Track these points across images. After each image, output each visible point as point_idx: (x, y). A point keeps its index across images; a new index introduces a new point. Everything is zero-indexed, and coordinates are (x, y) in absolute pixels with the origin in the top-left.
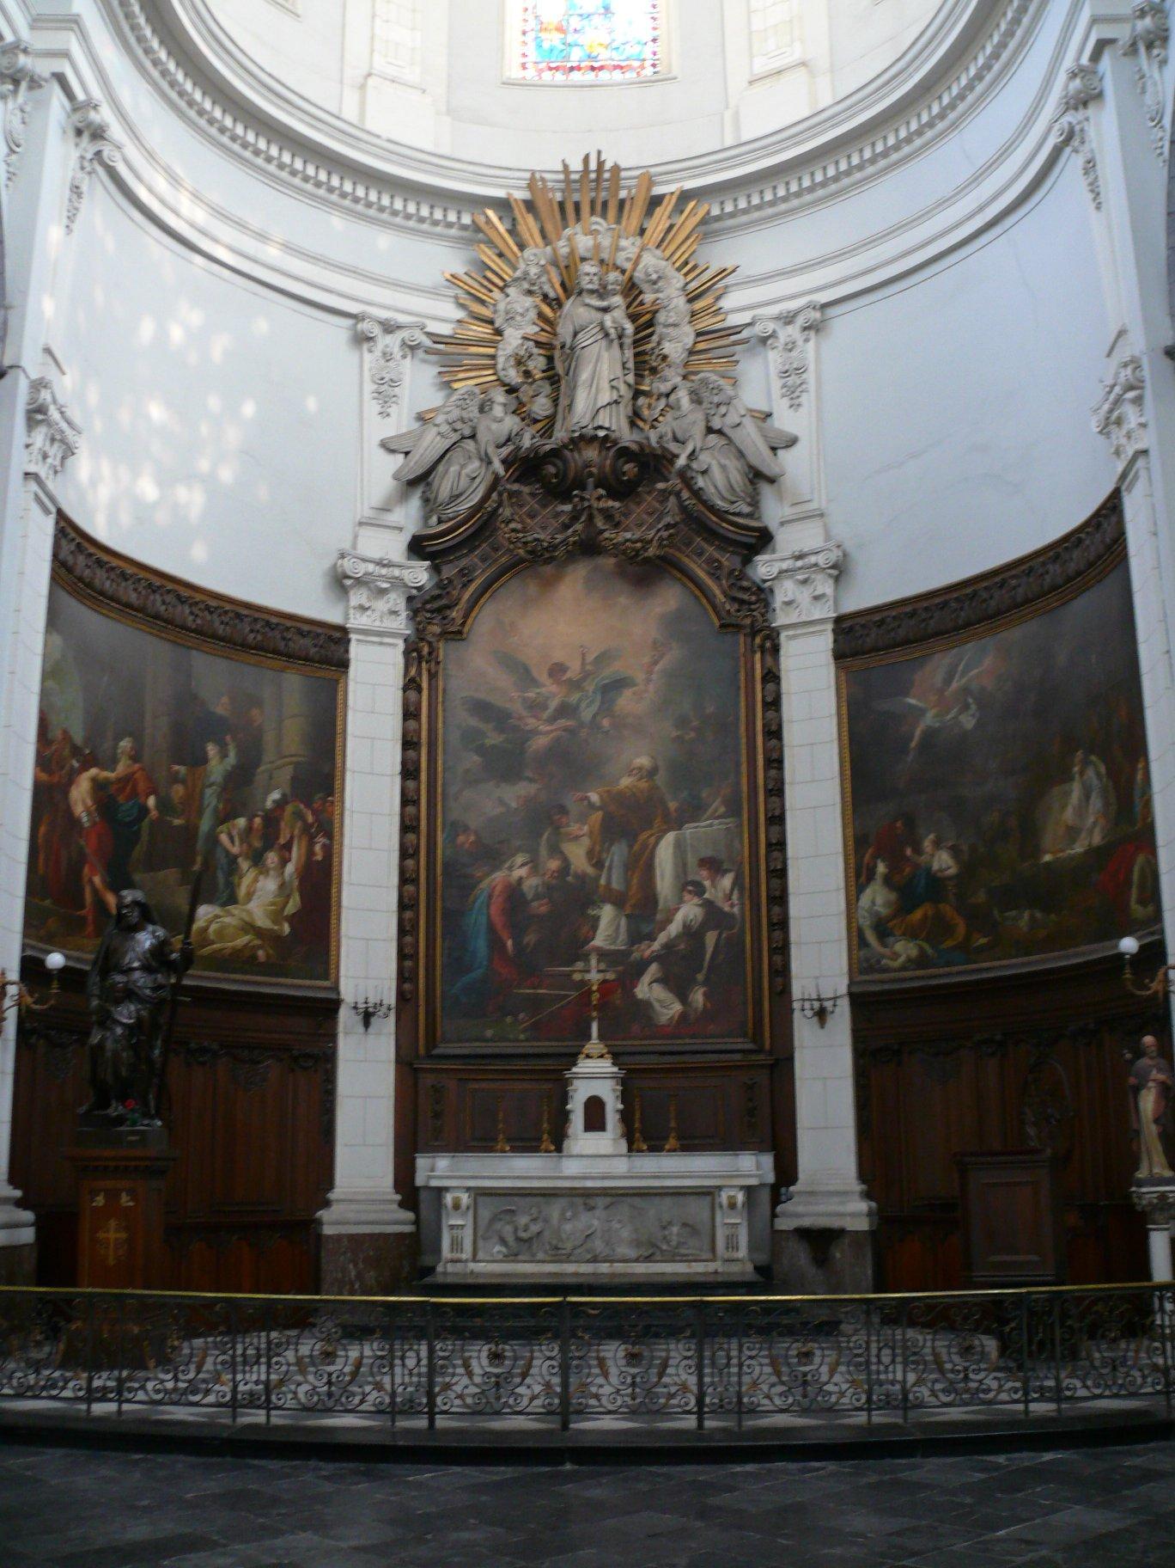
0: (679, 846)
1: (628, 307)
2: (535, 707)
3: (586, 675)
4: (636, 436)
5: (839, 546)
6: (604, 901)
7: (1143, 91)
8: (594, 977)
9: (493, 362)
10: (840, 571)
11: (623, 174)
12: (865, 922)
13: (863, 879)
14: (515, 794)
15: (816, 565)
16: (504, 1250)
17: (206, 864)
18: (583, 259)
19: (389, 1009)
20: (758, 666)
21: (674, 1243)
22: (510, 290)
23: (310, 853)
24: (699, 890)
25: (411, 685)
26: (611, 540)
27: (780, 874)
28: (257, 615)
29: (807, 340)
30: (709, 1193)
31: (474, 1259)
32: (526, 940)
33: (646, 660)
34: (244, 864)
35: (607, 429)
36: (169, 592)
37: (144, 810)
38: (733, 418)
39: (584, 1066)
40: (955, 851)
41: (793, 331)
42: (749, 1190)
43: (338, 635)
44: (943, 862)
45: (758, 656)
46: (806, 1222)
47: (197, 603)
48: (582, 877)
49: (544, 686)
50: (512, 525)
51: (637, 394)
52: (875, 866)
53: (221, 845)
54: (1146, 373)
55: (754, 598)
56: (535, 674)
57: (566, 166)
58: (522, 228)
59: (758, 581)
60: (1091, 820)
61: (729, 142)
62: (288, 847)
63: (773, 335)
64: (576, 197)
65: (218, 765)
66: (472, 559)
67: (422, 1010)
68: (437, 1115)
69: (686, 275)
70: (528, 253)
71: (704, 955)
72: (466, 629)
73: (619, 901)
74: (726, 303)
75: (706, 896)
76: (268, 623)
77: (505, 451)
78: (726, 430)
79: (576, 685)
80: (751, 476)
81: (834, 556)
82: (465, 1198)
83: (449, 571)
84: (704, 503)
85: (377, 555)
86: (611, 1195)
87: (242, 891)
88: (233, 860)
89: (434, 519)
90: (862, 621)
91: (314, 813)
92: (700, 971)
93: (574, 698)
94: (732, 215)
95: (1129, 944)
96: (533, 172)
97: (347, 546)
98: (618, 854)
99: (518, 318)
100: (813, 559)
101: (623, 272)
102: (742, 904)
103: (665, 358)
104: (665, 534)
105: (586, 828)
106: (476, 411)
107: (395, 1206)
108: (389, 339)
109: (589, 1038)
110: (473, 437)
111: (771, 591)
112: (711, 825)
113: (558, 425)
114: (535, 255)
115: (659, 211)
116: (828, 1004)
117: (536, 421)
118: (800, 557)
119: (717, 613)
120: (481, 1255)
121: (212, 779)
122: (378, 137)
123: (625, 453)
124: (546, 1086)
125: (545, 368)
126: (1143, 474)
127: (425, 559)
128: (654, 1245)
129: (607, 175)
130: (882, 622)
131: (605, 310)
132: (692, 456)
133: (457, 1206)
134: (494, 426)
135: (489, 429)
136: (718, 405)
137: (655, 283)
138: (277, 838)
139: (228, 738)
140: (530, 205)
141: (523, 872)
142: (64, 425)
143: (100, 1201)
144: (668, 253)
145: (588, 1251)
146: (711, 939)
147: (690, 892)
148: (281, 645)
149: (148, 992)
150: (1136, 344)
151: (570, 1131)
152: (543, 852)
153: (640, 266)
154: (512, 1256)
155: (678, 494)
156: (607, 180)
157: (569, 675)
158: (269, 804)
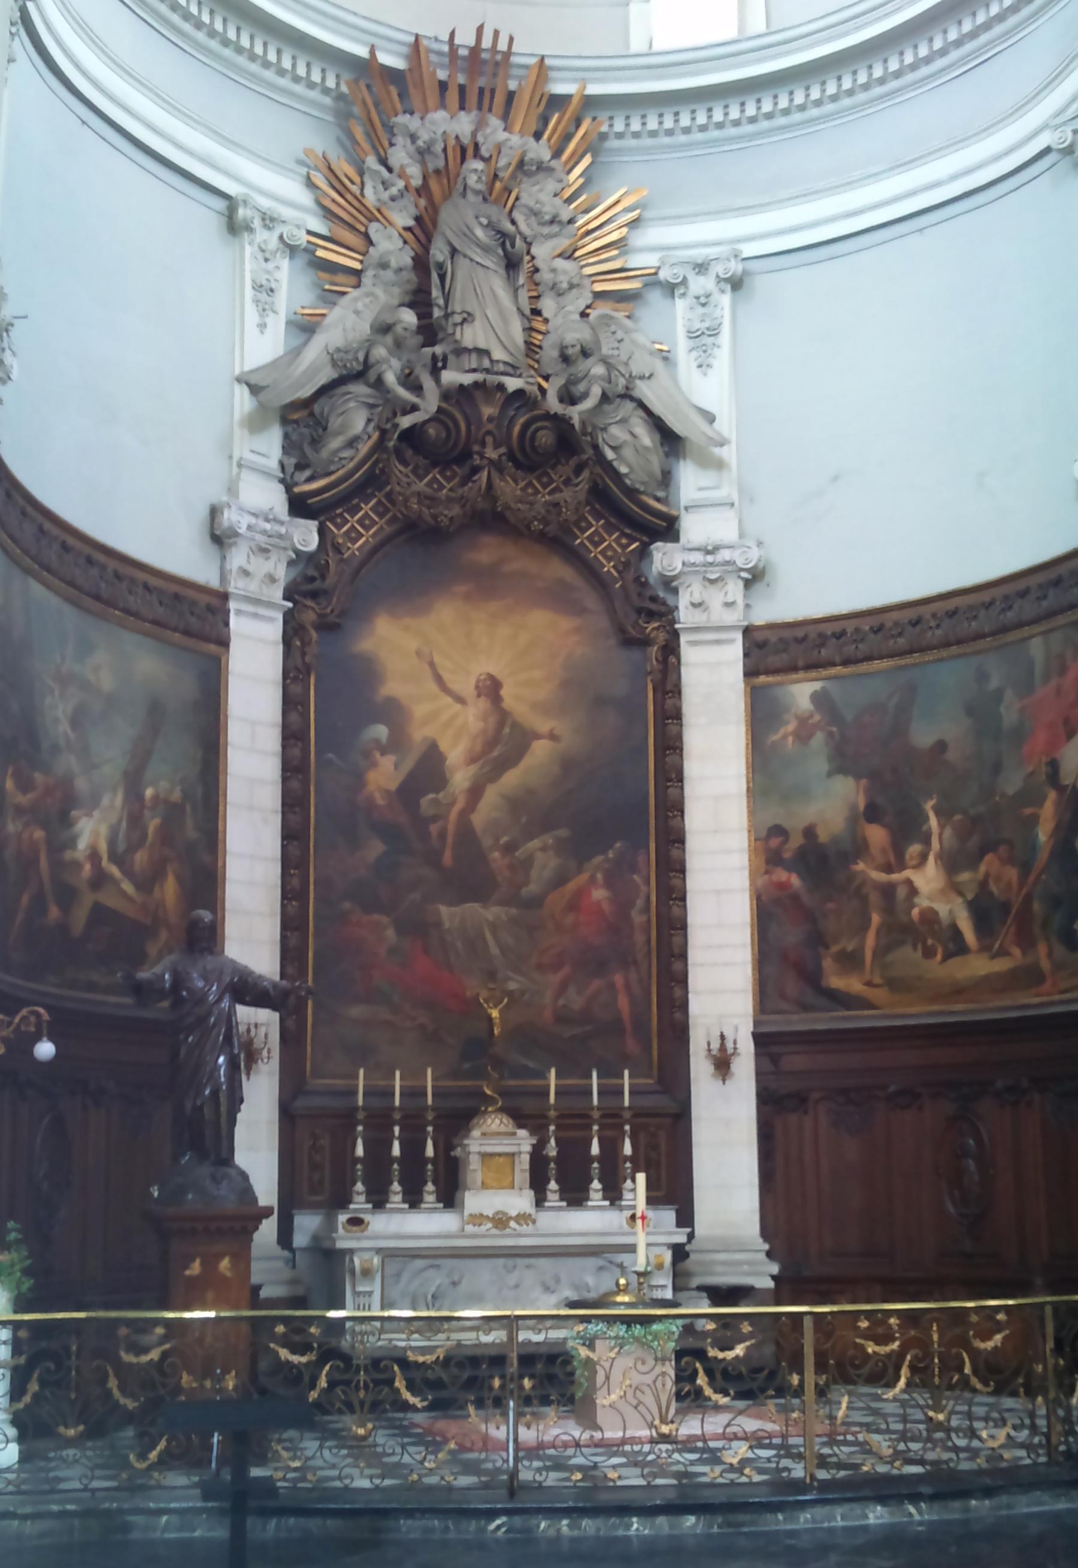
15: (727, 563)
96: (417, 36)
100: (725, 555)
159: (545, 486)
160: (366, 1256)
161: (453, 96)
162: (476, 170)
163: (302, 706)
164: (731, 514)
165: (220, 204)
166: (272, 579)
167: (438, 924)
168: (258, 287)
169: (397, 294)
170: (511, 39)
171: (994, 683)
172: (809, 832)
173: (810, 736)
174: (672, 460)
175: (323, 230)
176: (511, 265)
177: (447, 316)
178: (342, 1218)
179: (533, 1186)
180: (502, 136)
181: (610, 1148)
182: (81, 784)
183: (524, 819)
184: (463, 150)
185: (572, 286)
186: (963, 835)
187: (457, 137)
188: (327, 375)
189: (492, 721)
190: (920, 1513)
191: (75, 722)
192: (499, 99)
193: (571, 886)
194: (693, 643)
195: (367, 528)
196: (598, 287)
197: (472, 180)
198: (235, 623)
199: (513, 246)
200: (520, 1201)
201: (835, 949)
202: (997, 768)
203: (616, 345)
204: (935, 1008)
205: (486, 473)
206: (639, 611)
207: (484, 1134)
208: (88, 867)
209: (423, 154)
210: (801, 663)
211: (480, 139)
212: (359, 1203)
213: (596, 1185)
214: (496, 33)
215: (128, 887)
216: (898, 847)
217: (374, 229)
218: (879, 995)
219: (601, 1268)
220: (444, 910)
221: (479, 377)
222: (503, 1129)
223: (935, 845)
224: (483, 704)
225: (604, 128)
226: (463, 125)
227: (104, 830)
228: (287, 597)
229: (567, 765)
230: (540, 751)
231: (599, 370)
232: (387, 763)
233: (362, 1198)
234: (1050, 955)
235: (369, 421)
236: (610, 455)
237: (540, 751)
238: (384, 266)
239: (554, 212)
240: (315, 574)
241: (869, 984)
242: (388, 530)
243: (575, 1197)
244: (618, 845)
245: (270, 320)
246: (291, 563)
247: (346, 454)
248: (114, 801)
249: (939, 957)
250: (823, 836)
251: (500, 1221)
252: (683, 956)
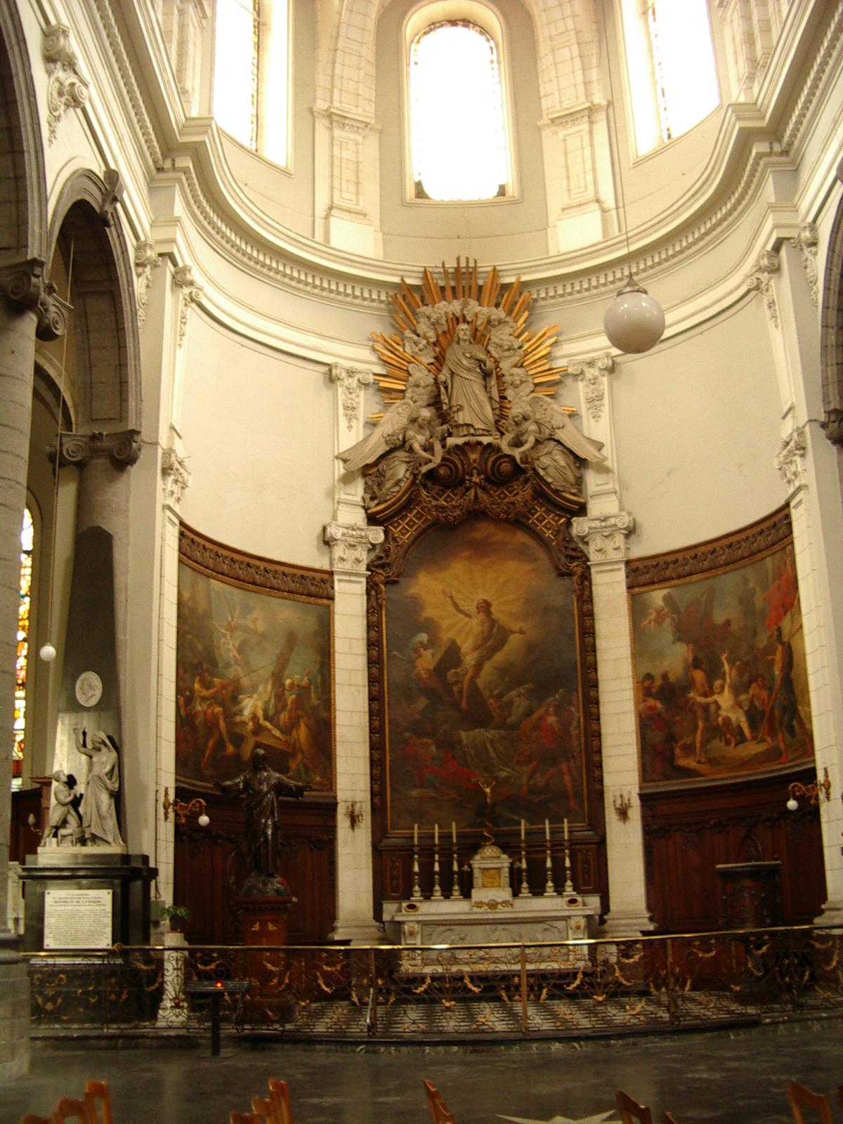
15: (615, 525)
81: (625, 521)
96: (425, 267)
100: (612, 521)
118: (605, 519)
159: (510, 492)
160: (411, 925)
161: (449, 293)
162: (463, 330)
163: (377, 627)
164: (614, 497)
165: (324, 369)
166: (358, 561)
167: (460, 741)
168: (346, 408)
169: (424, 399)
170: (476, 261)
171: (751, 585)
172: (665, 676)
173: (664, 620)
174: (583, 470)
175: (384, 372)
176: (486, 375)
177: (450, 408)
178: (405, 905)
179: (511, 886)
180: (478, 309)
181: (558, 862)
182: (245, 682)
183: (507, 680)
184: (457, 319)
185: (522, 382)
186: (741, 673)
187: (453, 314)
188: (384, 448)
189: (486, 625)
190: (581, 1047)
191: (240, 650)
193: (535, 716)
194: (598, 572)
195: (411, 527)
196: (537, 381)
197: (461, 335)
198: (337, 585)
199: (485, 365)
200: (505, 894)
201: (681, 743)
202: (755, 633)
203: (544, 412)
204: (733, 774)
205: (473, 491)
206: (567, 556)
207: (482, 858)
208: (251, 724)
209: (434, 325)
210: (655, 580)
211: (465, 312)
212: (417, 895)
213: (550, 884)
214: (467, 259)
215: (277, 733)
216: (710, 681)
217: (411, 368)
218: (704, 768)
219: (545, 930)
220: (463, 734)
221: (466, 439)
222: (493, 854)
223: (728, 680)
224: (481, 616)
225: (535, 296)
226: (455, 307)
227: (260, 704)
228: (368, 569)
229: (530, 648)
230: (515, 641)
231: (533, 427)
232: (427, 654)
233: (418, 894)
234: (784, 740)
235: (407, 470)
236: (542, 473)
237: (515, 641)
238: (418, 386)
239: (510, 344)
240: (383, 555)
241: (699, 762)
242: (423, 526)
243: (538, 891)
244: (561, 691)
245: (354, 423)
246: (369, 551)
247: (396, 489)
248: (266, 689)
249: (733, 744)
250: (672, 678)
251: (493, 905)
252: (600, 752)
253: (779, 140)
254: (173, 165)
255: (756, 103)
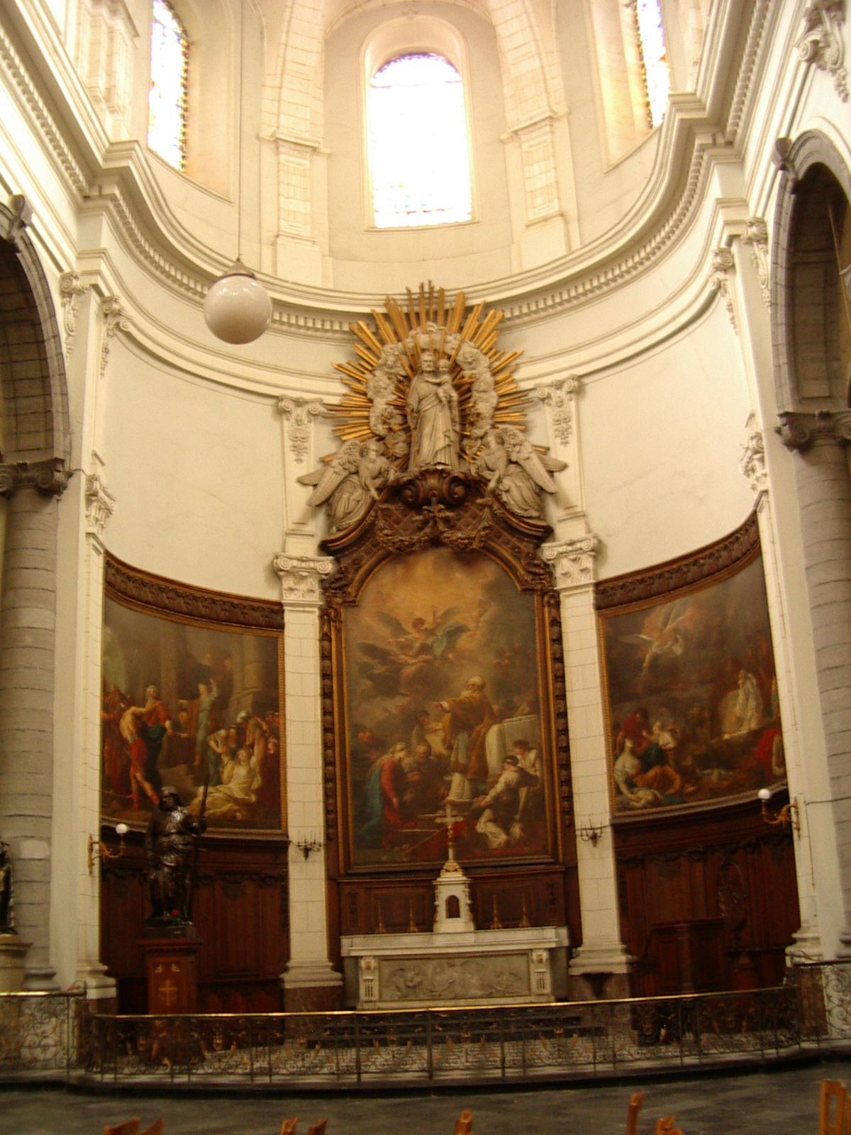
0: (501, 735)
1: (454, 379)
2: (405, 647)
3: (437, 625)
4: (464, 469)
5: (594, 537)
6: (454, 771)
7: (758, 266)
8: (449, 821)
9: (367, 421)
10: (598, 552)
11: (447, 293)
12: (620, 778)
13: (617, 751)
14: (394, 705)
15: (581, 549)
16: (399, 994)
17: (202, 761)
18: (423, 350)
19: (320, 846)
20: (547, 615)
21: (505, 986)
22: (377, 373)
23: (266, 749)
24: (514, 761)
25: (325, 637)
26: (448, 538)
27: (566, 749)
28: (225, 599)
29: (571, 400)
30: (525, 953)
31: (381, 1001)
32: (405, 798)
33: (475, 614)
34: (225, 759)
35: (444, 464)
36: (170, 590)
37: (164, 729)
38: (524, 454)
39: (445, 877)
40: (673, 732)
41: (562, 394)
42: (551, 950)
43: (276, 608)
44: (666, 739)
45: (546, 609)
46: (588, 970)
47: (187, 596)
48: (439, 756)
49: (409, 633)
50: (386, 532)
51: (463, 437)
52: (624, 743)
53: (210, 747)
54: (764, 443)
55: (542, 571)
56: (404, 626)
57: (408, 290)
58: (382, 331)
59: (544, 559)
60: (749, 713)
61: (516, 271)
62: (252, 746)
63: (549, 397)
64: (416, 309)
65: (207, 697)
66: (362, 552)
67: (341, 845)
68: (353, 912)
69: (490, 358)
70: (387, 348)
71: (519, 803)
72: (358, 599)
73: (464, 771)
74: (517, 376)
75: (519, 765)
76: (232, 604)
77: (379, 482)
78: (521, 462)
79: (431, 632)
80: (537, 491)
81: (593, 542)
82: (373, 963)
83: (346, 562)
84: (508, 511)
85: (298, 554)
86: (465, 957)
87: (225, 776)
88: (218, 756)
89: (334, 529)
90: (611, 585)
91: (268, 723)
92: (516, 813)
93: (430, 641)
94: (518, 317)
95: (764, 794)
97: (278, 550)
98: (462, 740)
99: (382, 391)
100: (578, 545)
101: (449, 357)
102: (543, 769)
103: (478, 415)
104: (483, 533)
105: (440, 725)
106: (358, 454)
107: (329, 970)
108: (299, 410)
109: (447, 858)
110: (357, 473)
111: (554, 566)
112: (521, 720)
113: (411, 462)
114: (391, 349)
115: (471, 316)
116: (598, 831)
117: (397, 458)
118: (571, 544)
119: (520, 582)
120: (384, 997)
121: (203, 706)
122: (287, 282)
123: (456, 480)
124: (421, 891)
125: (401, 422)
126: (765, 505)
127: (329, 555)
128: (491, 987)
129: (436, 295)
130: (624, 586)
131: (439, 385)
132: (499, 481)
133: (368, 968)
134: (371, 466)
135: (367, 468)
136: (514, 445)
137: (470, 363)
138: (245, 741)
139: (211, 681)
140: (387, 317)
141: (401, 755)
142: (106, 499)
143: (160, 969)
144: (477, 345)
145: (451, 993)
146: (523, 792)
147: (508, 763)
148: (241, 618)
149: (180, 846)
150: (760, 425)
151: (438, 919)
152: (414, 740)
153: (461, 353)
154: (404, 998)
155: (490, 507)
156: (436, 298)
157: (426, 626)
158: (239, 720)
192: (441, 313)
253: (723, 132)
254: (100, 191)
255: (694, 94)
